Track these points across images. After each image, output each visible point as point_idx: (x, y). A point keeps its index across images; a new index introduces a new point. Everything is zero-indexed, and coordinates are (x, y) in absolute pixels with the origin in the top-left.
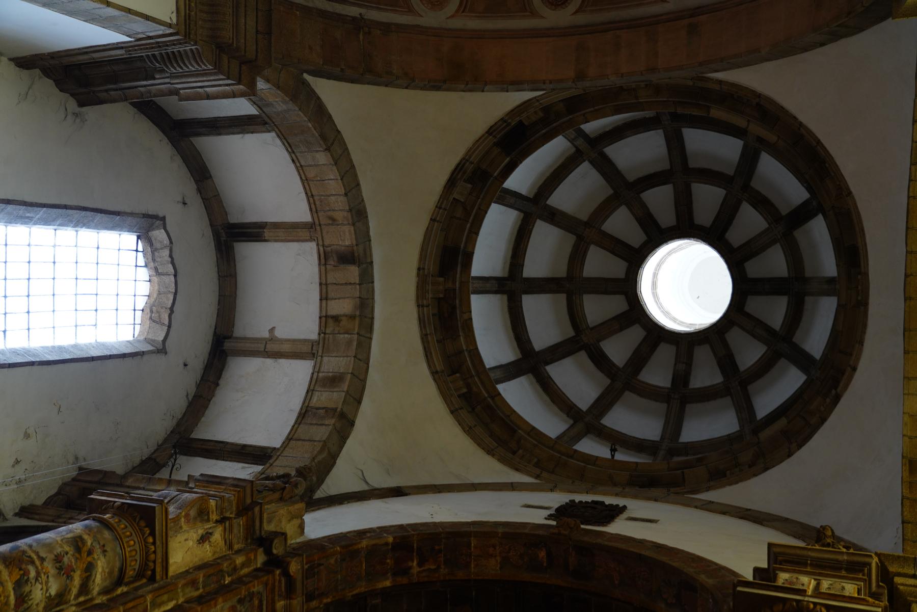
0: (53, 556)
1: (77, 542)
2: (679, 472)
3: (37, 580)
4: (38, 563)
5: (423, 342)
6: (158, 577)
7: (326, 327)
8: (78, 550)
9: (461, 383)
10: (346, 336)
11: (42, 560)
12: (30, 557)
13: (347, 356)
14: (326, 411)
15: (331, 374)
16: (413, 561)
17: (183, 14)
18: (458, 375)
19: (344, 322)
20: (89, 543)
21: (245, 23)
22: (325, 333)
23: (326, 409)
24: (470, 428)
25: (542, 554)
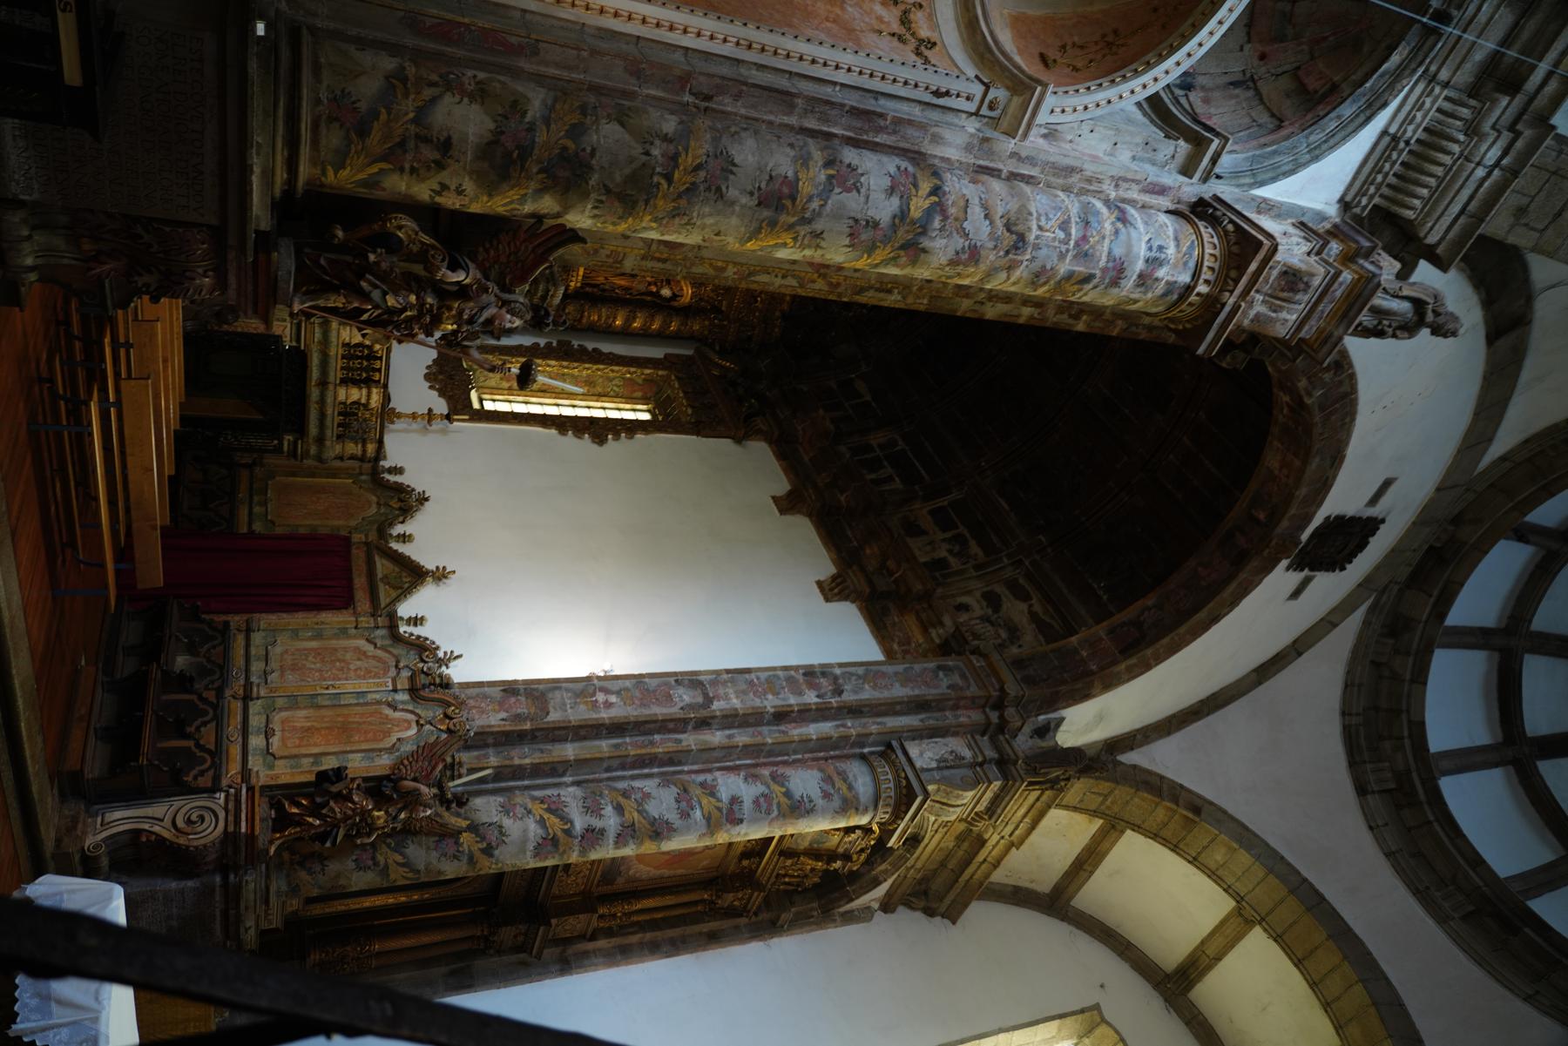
2: (1436, 593)
25: (1262, 516)
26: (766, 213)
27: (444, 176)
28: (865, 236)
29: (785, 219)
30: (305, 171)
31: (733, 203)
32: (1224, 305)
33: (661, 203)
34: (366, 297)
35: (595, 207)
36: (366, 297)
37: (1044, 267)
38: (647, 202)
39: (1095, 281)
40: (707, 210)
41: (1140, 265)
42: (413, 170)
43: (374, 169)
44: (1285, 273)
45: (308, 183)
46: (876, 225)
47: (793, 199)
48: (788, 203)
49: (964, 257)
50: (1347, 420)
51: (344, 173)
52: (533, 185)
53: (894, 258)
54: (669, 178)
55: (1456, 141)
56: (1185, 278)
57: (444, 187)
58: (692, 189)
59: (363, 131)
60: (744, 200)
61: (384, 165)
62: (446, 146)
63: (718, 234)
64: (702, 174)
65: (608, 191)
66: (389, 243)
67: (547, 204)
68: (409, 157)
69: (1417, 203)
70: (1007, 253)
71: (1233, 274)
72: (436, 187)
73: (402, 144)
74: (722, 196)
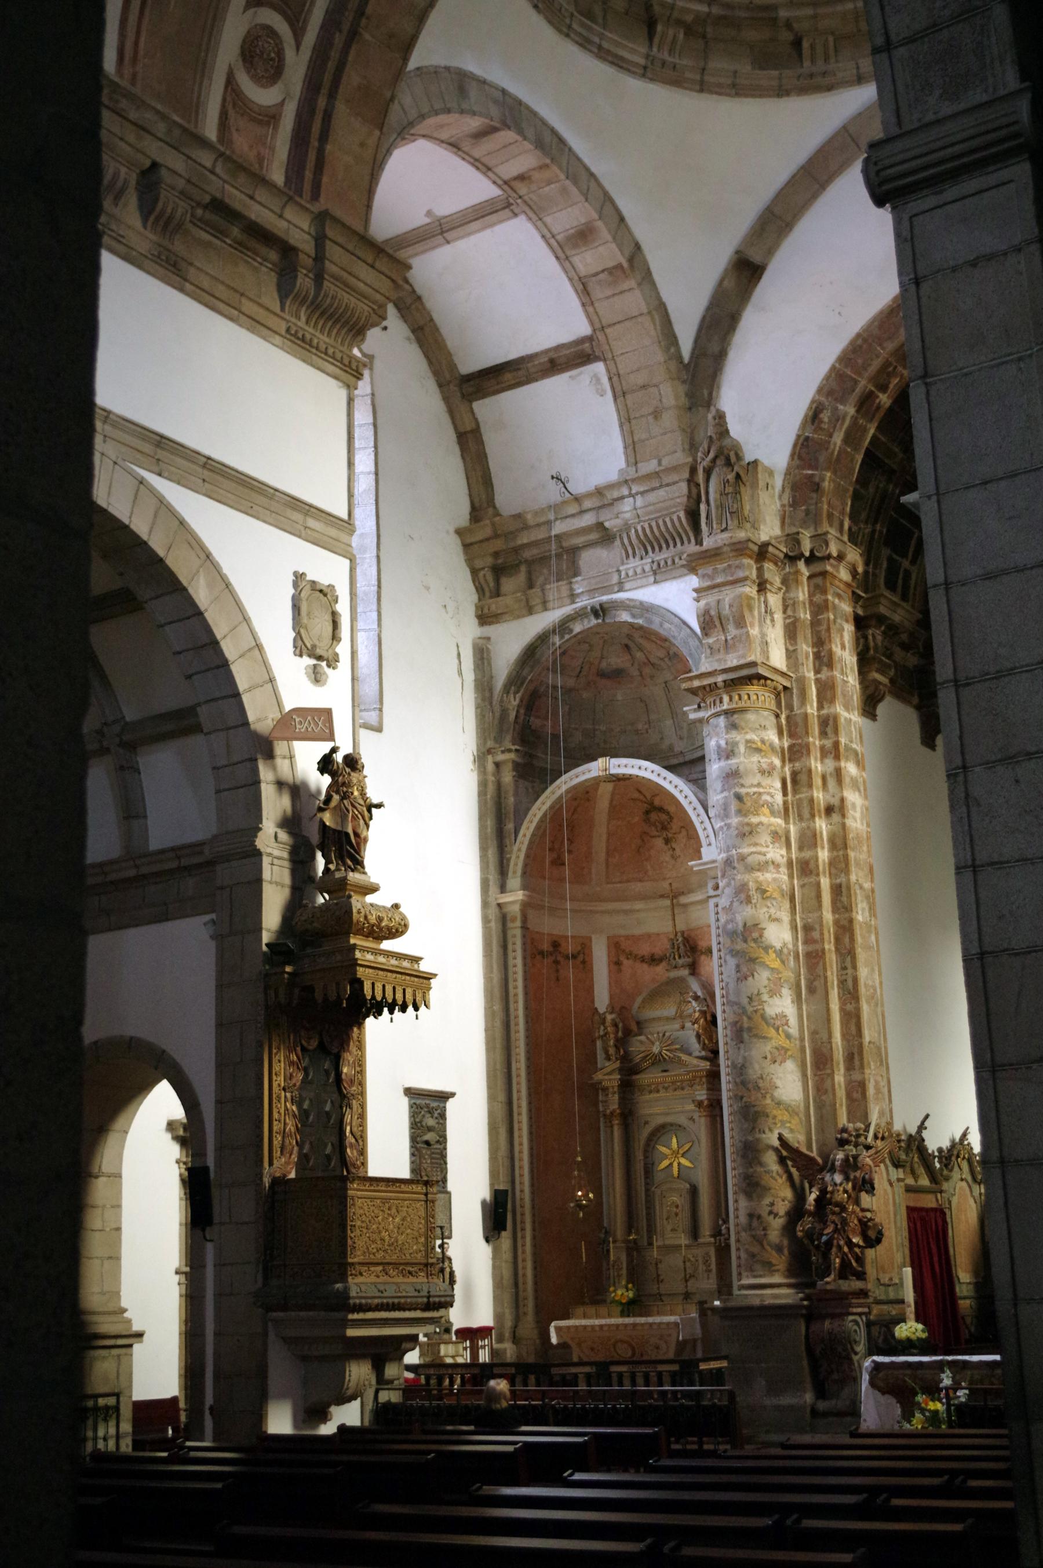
0: (759, 775)
1: (750, 747)
3: (772, 796)
4: (761, 790)
5: (604, 59)
6: (787, 684)
7: (515, 192)
8: (758, 750)
9: (671, 32)
10: (553, 186)
11: (759, 785)
12: (754, 793)
13: (575, 204)
14: (611, 273)
15: (572, 231)
16: (878, 397)
17: (338, 371)
18: (659, 28)
19: (536, 175)
20: (756, 738)
21: (366, 284)
22: (520, 197)
23: (610, 271)
24: (734, 85)
26: (745, 1036)
27: (764, 1213)
28: (744, 969)
29: (746, 1025)
30: (777, 1279)
31: (745, 1058)
32: (725, 681)
33: (753, 1098)
34: (829, 1244)
35: (764, 1132)
36: (829, 1244)
37: (737, 836)
38: (754, 1106)
39: (737, 789)
40: (751, 1071)
41: (723, 763)
42: (765, 1229)
43: (768, 1248)
44: (706, 635)
45: (787, 1277)
46: (738, 966)
47: (737, 1022)
48: (738, 1025)
49: (743, 896)
50: (859, 342)
51: (774, 1262)
52: (759, 1169)
53: (755, 940)
54: (742, 1098)
55: (636, 531)
56: (722, 721)
57: (770, 1213)
58: (744, 1083)
59: (753, 1256)
60: (742, 1052)
61: (765, 1243)
62: (751, 1216)
63: (766, 1058)
64: (738, 1080)
65: (754, 1128)
66: (810, 1234)
67: (770, 1160)
68: (758, 1232)
69: (675, 518)
70: (734, 868)
71: (708, 689)
72: (772, 1217)
73: (754, 1237)
74: (743, 1065)
